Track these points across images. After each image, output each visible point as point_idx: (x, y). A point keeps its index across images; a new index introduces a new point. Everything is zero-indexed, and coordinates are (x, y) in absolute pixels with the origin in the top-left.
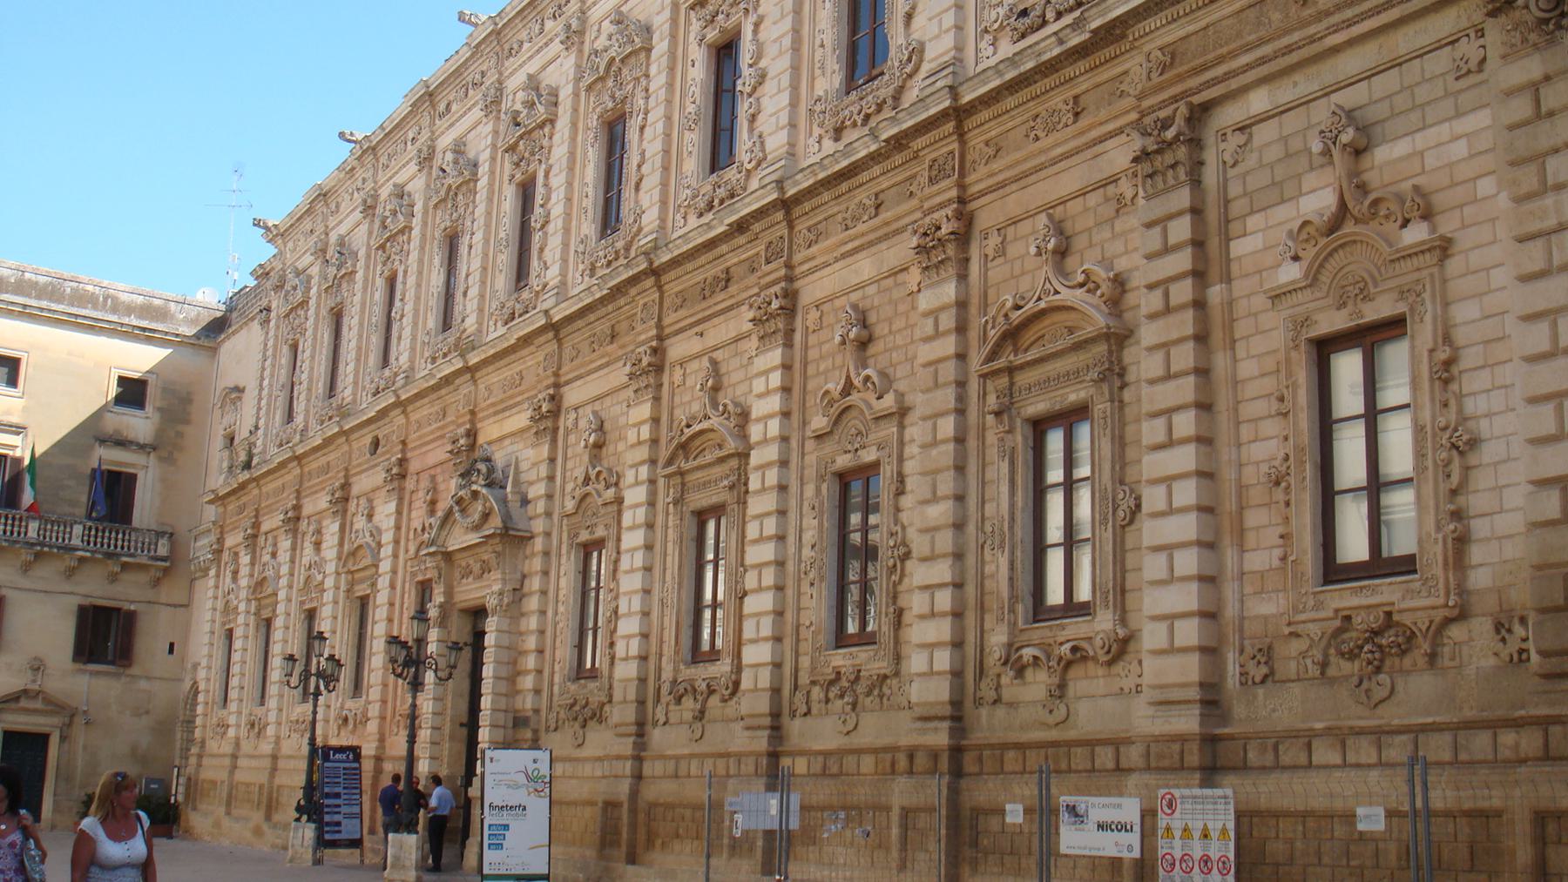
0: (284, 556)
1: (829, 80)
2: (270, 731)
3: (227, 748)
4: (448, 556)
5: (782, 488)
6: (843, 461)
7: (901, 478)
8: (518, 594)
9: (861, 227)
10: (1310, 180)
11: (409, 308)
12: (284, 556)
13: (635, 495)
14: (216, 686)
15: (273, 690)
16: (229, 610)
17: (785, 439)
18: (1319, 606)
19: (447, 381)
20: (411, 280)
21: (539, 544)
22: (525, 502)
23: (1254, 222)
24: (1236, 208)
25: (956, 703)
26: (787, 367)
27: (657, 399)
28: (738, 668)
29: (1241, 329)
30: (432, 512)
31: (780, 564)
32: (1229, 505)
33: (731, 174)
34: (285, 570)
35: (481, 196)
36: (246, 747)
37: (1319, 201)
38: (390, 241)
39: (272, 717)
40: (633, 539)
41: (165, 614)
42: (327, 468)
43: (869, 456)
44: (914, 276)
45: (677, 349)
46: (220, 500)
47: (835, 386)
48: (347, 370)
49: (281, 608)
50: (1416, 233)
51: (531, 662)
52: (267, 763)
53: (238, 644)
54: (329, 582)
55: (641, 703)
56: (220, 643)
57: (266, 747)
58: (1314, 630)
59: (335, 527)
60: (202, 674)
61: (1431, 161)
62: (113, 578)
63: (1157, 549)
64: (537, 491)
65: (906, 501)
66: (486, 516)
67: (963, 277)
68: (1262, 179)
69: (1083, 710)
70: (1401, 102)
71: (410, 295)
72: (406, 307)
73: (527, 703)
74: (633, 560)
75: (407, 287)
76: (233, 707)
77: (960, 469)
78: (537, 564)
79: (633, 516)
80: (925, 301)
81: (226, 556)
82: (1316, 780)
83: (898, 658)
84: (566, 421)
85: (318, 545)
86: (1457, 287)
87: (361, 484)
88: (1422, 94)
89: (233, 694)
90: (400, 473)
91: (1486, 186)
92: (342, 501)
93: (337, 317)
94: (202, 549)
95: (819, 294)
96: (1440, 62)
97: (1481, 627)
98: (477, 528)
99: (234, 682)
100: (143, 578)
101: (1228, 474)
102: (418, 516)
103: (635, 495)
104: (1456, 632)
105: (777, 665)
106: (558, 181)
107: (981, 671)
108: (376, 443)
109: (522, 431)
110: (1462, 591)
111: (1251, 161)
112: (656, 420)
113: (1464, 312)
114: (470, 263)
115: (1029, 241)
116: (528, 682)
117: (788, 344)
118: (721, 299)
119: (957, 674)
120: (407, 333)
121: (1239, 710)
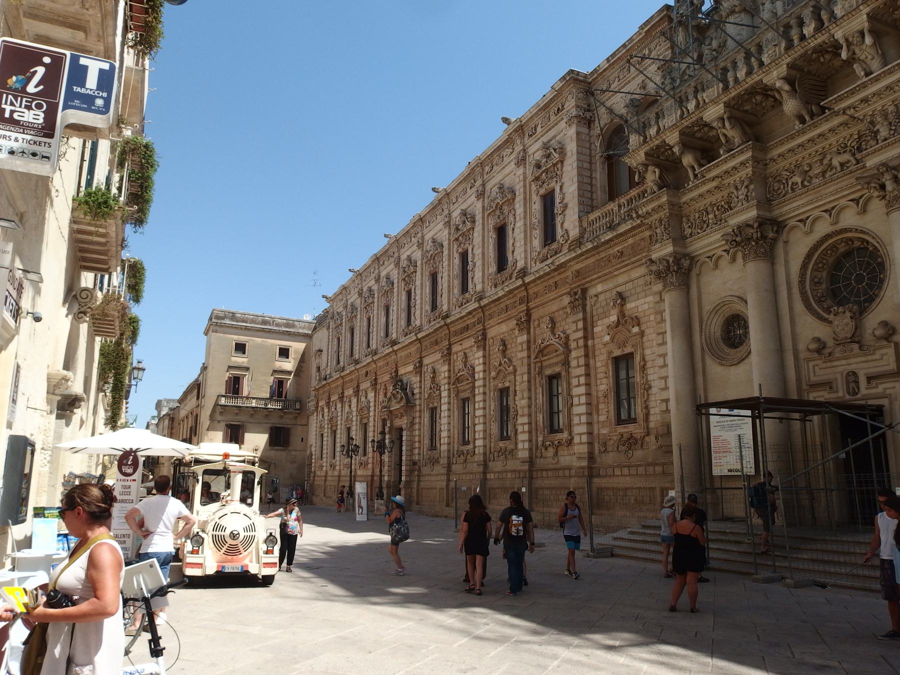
0: (339, 409)
1: (493, 268)
2: (337, 468)
3: (323, 474)
4: (391, 412)
5: (484, 393)
6: (500, 386)
7: (515, 391)
8: (412, 424)
9: (503, 316)
10: (612, 312)
11: (375, 329)
12: (339, 409)
13: (444, 394)
14: (318, 453)
15: (338, 454)
16: (322, 427)
17: (484, 378)
18: (616, 431)
19: (388, 354)
20: (375, 320)
21: (418, 408)
22: (413, 394)
23: (599, 323)
24: (595, 318)
25: (531, 458)
26: (484, 357)
27: (449, 364)
28: (475, 447)
29: (597, 353)
31: (485, 416)
32: (594, 402)
33: (467, 295)
34: (339, 414)
35: (395, 294)
36: (330, 473)
37: (614, 318)
38: (368, 306)
39: (338, 463)
40: (444, 407)
41: (299, 428)
42: (351, 381)
43: (507, 384)
45: (455, 348)
46: (316, 390)
47: (497, 364)
48: (356, 348)
49: (339, 427)
50: (636, 330)
51: (417, 445)
52: (337, 478)
53: (325, 439)
54: (354, 419)
55: (449, 458)
56: (319, 438)
57: (336, 473)
58: (615, 438)
60: (313, 449)
61: (640, 310)
62: (281, 417)
63: (577, 415)
64: (416, 391)
65: (517, 398)
66: (402, 398)
69: (562, 459)
71: (375, 325)
72: (374, 329)
73: (416, 458)
74: (445, 414)
75: (374, 322)
76: (325, 460)
77: (530, 390)
78: (418, 414)
79: (444, 400)
82: (615, 480)
83: (516, 444)
84: (424, 369)
85: (350, 406)
86: (646, 344)
87: (363, 386)
89: (324, 456)
90: (375, 384)
92: (357, 392)
93: (352, 331)
94: (311, 405)
97: (653, 437)
98: (399, 403)
99: (324, 451)
100: (291, 416)
101: (594, 394)
102: (381, 397)
103: (444, 394)
104: (647, 439)
105: (485, 446)
106: (418, 292)
107: (537, 448)
108: (367, 373)
109: (411, 372)
110: (648, 428)
111: (598, 305)
112: (449, 371)
113: (648, 352)
114: (393, 316)
116: (416, 451)
117: (484, 349)
118: (466, 334)
119: (530, 449)
120: (375, 337)
121: (598, 460)
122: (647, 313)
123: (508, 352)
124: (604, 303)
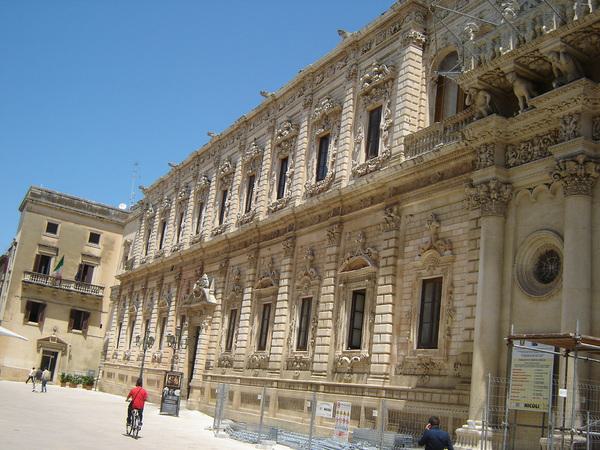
10: (426, 233)
23: (411, 243)
24: (408, 238)
30: (188, 293)
42: (157, 273)
44: (327, 242)
50: (448, 252)
59: (157, 293)
67: (338, 246)
68: (414, 231)
70: (449, 215)
80: (329, 251)
81: (122, 298)
87: (167, 280)
88: (454, 214)
91: (465, 243)
95: (303, 244)
96: (459, 206)
115: (357, 241)
122: (462, 238)
123: (316, 262)
124: (418, 224)
